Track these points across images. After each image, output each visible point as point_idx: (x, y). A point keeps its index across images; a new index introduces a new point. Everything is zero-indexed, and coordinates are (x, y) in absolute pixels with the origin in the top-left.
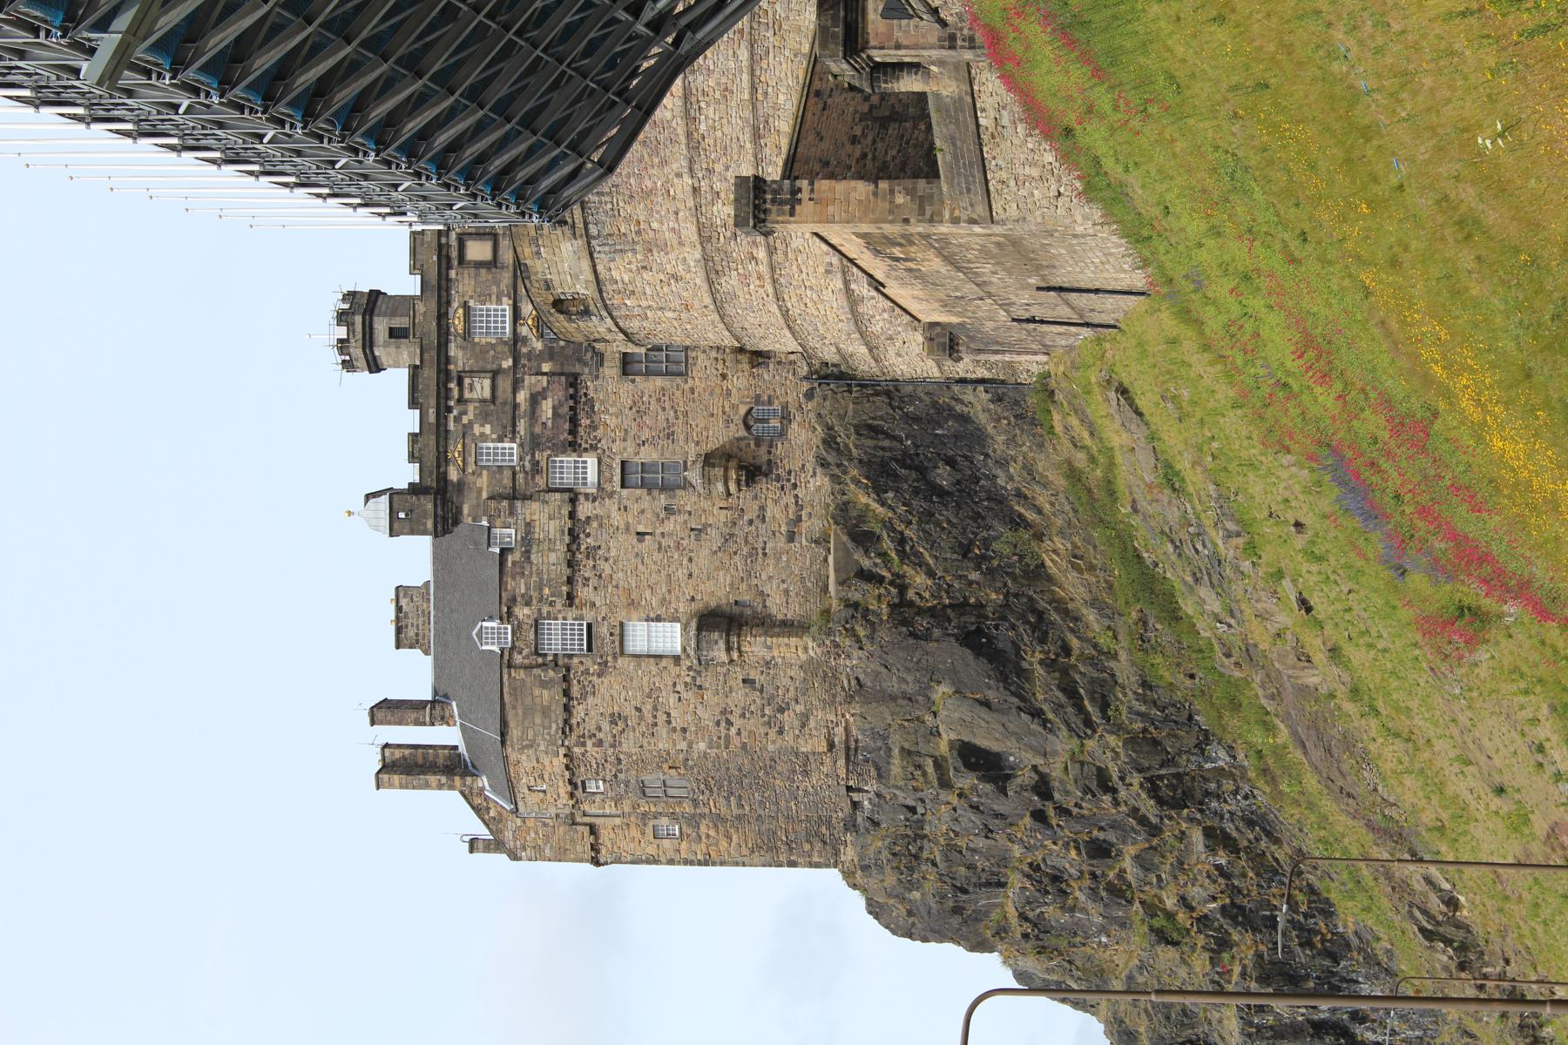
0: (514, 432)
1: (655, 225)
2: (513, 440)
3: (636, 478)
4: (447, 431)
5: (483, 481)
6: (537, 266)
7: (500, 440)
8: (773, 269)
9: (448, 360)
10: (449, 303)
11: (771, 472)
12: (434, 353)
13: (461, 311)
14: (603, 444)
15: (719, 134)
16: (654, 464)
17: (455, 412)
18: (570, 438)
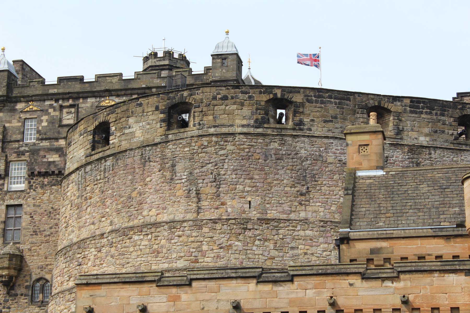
0: (42, 139)
1: (89, 209)
2: (38, 139)
3: (12, 213)
4: (44, 100)
5: (16, 124)
6: (77, 136)
7: (38, 132)
8: (62, 292)
9: (85, 98)
10: (118, 96)
11: (10, 296)
12: (89, 89)
13: (113, 103)
14: (33, 193)
15: (131, 249)
16: (20, 224)
17: (55, 104)
18: (36, 173)
